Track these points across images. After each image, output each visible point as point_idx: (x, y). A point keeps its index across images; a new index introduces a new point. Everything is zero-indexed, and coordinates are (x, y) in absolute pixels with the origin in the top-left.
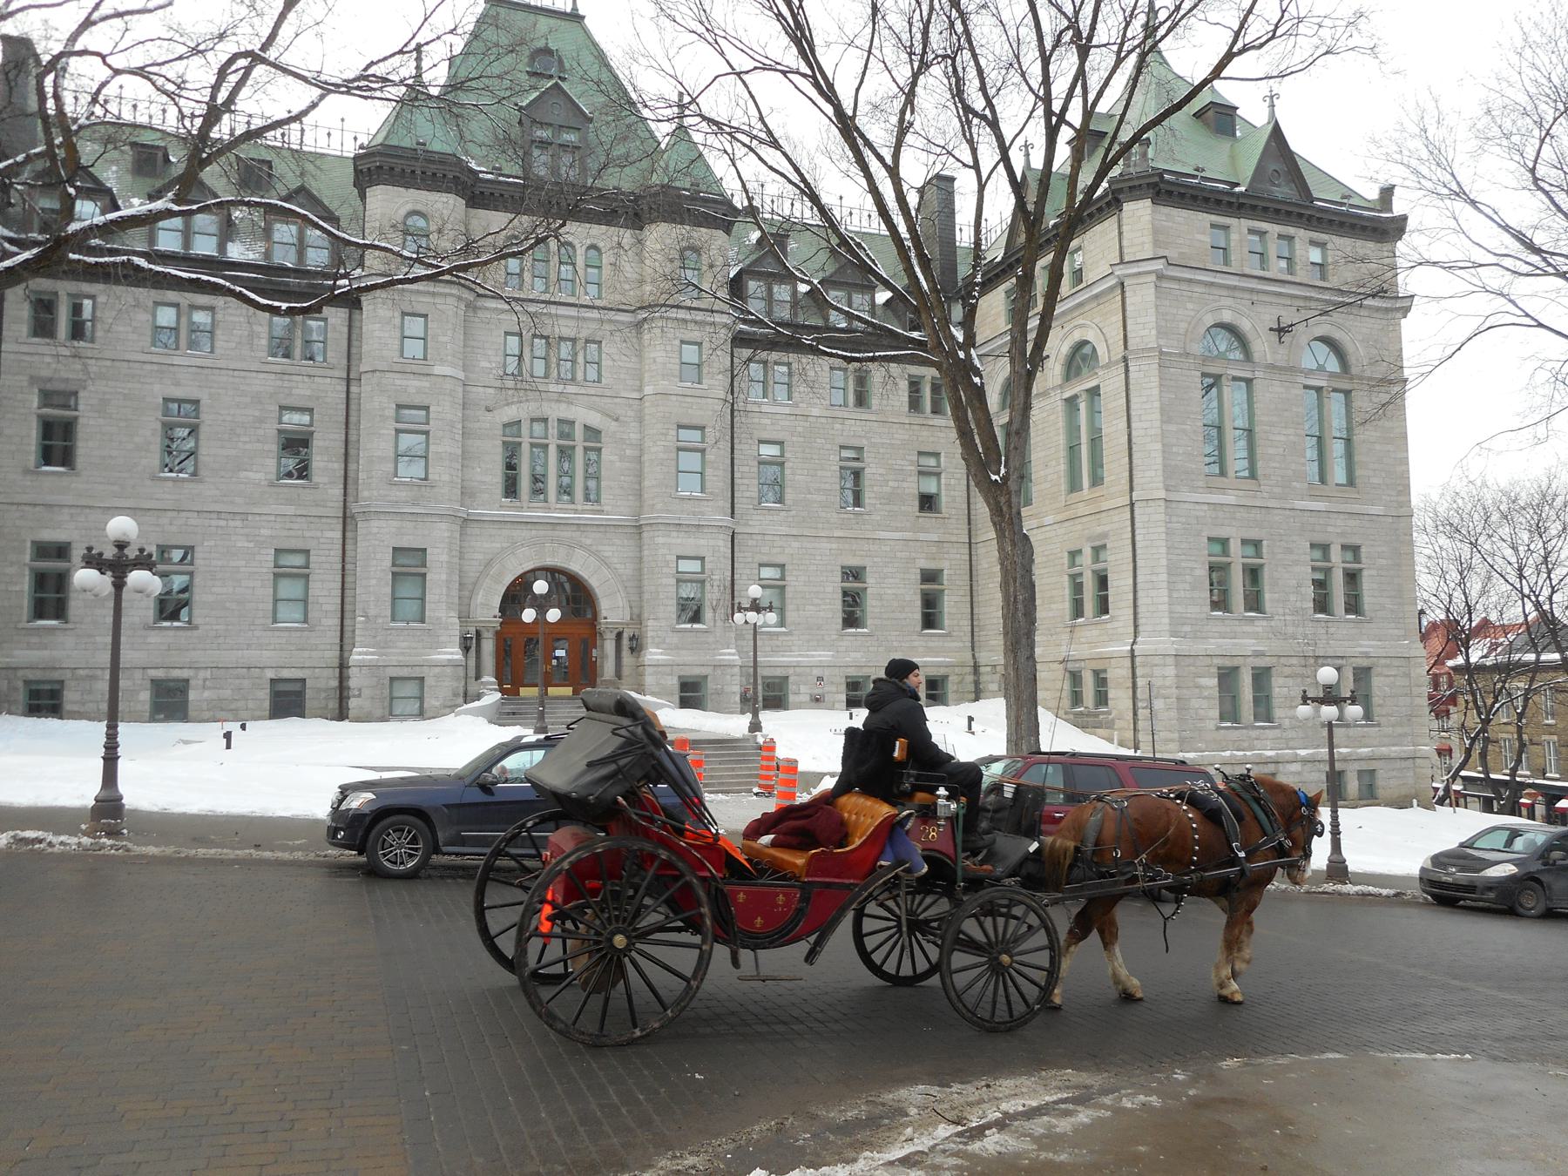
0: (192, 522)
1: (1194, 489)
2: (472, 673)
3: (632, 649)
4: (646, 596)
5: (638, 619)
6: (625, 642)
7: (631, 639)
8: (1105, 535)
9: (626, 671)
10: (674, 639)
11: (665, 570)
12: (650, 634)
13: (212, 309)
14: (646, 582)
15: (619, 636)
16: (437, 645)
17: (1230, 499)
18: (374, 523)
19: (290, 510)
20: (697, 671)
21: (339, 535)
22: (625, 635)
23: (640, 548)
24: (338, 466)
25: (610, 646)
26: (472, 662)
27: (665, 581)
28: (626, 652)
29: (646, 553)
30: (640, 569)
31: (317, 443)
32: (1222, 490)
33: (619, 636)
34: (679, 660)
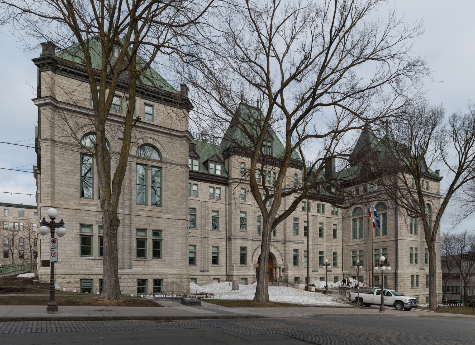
0: (196, 239)
1: (408, 237)
5: (285, 263)
8: (387, 246)
10: (293, 269)
13: (197, 185)
16: (249, 270)
17: (413, 239)
18: (237, 241)
19: (215, 237)
20: (298, 276)
21: (225, 243)
23: (285, 247)
24: (224, 226)
31: (220, 220)
32: (412, 237)
34: (295, 274)
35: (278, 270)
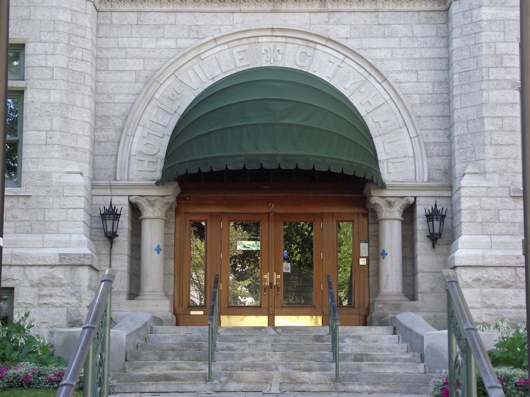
2: (121, 283)
3: (434, 238)
4: (458, 130)
6: (421, 225)
7: (430, 217)
9: (424, 282)
11: (494, 74)
12: (465, 204)
14: (456, 104)
15: (409, 211)
22: (420, 211)
25: (392, 234)
26: (121, 263)
27: (494, 96)
28: (422, 244)
29: (456, 43)
30: (448, 83)
33: (409, 211)
35: (392, 234)
